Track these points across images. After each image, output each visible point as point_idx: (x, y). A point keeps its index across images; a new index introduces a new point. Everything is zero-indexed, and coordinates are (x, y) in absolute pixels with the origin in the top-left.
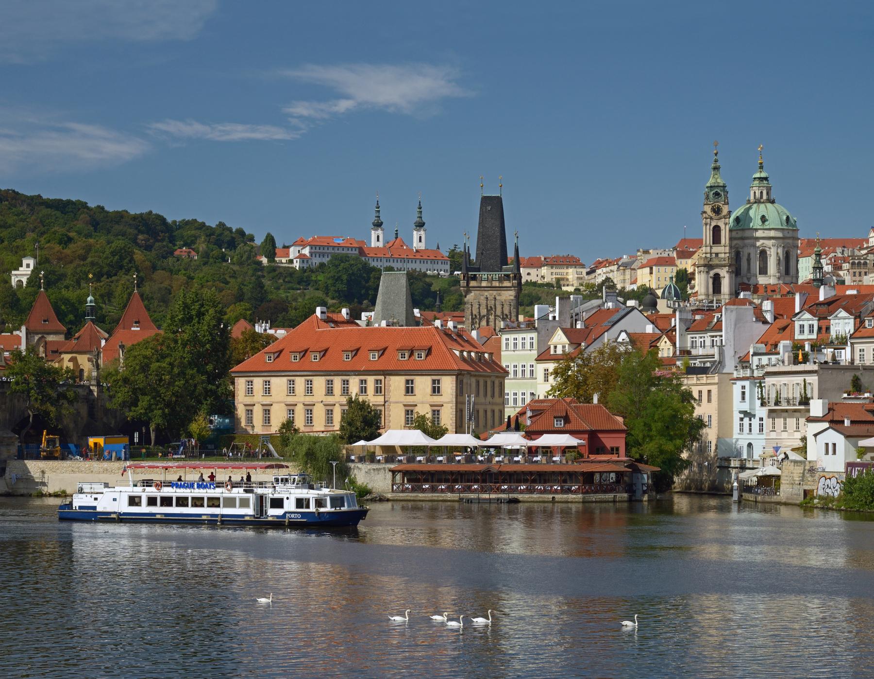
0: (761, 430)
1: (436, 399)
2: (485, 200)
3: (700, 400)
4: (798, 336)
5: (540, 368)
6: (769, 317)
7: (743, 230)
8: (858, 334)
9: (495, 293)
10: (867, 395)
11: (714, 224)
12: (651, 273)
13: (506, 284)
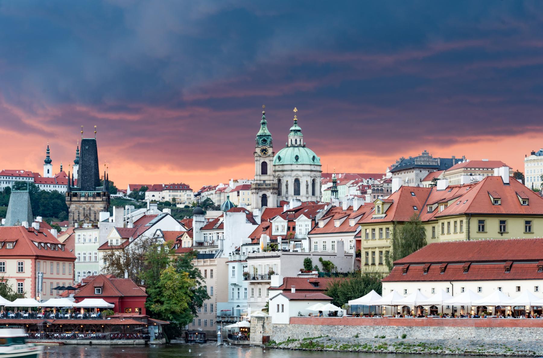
0: (246, 296)
1: (21, 275)
2: (84, 142)
3: (206, 276)
4: (274, 233)
5: (101, 254)
6: (258, 220)
7: (283, 165)
8: (313, 232)
9: (90, 205)
10: (314, 272)
11: (262, 161)
12: (238, 195)
13: (98, 199)
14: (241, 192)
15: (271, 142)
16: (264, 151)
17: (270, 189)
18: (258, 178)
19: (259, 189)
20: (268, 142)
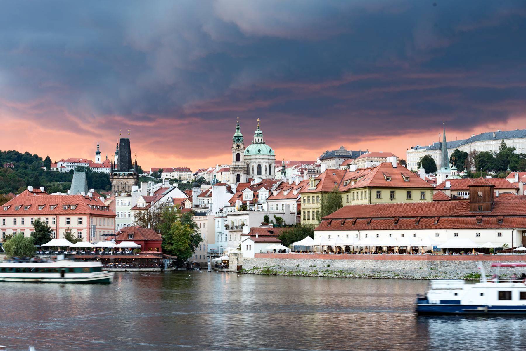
0: (226, 240)
1: (80, 227)
2: (122, 140)
3: (201, 227)
4: (244, 199)
5: (133, 213)
6: (234, 191)
8: (270, 198)
9: (125, 181)
10: (270, 224)
12: (222, 175)
13: (131, 177)
14: (223, 173)
15: (243, 141)
16: (238, 146)
17: (242, 171)
18: (234, 164)
19: (235, 171)
20: (241, 140)
